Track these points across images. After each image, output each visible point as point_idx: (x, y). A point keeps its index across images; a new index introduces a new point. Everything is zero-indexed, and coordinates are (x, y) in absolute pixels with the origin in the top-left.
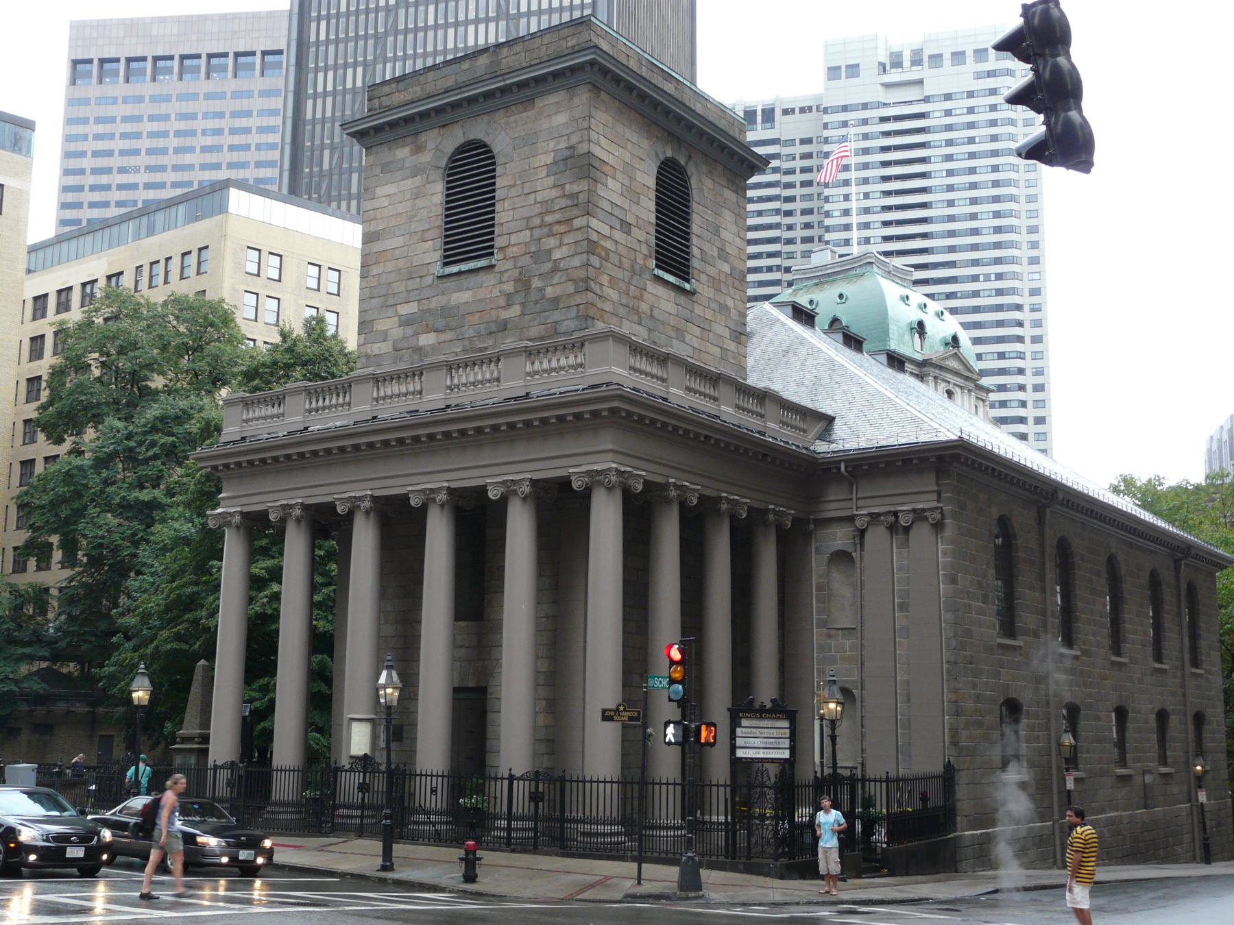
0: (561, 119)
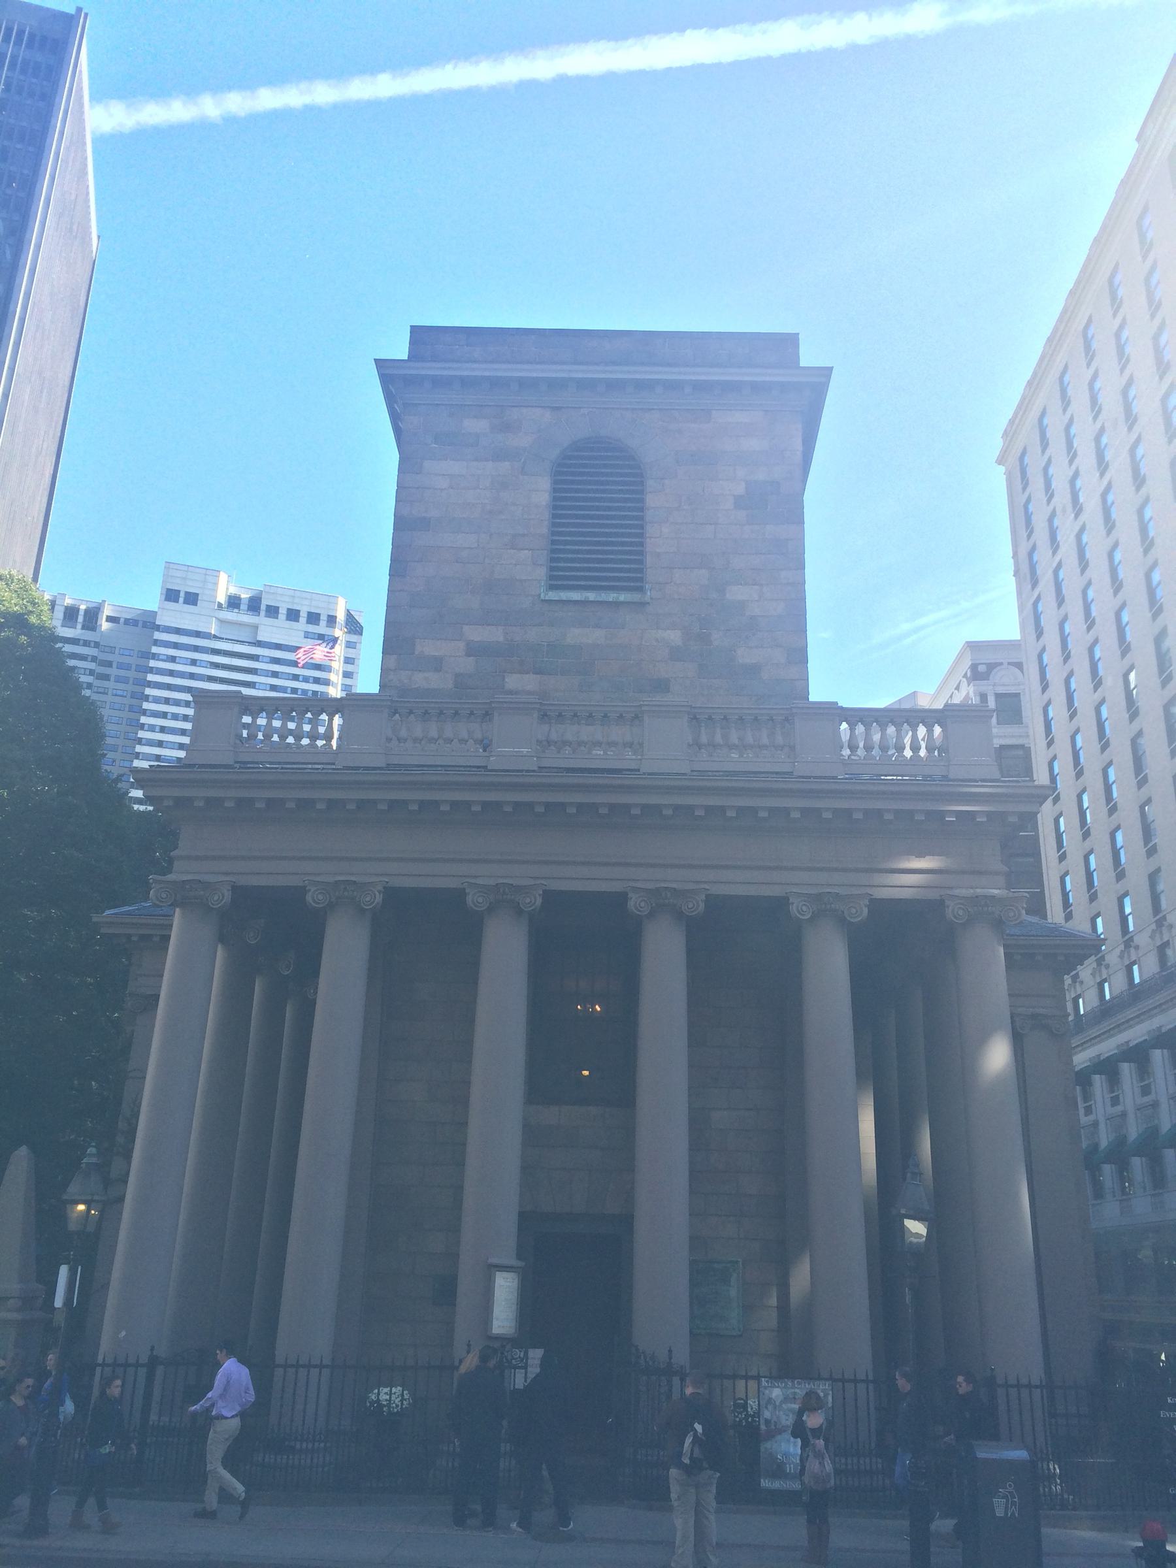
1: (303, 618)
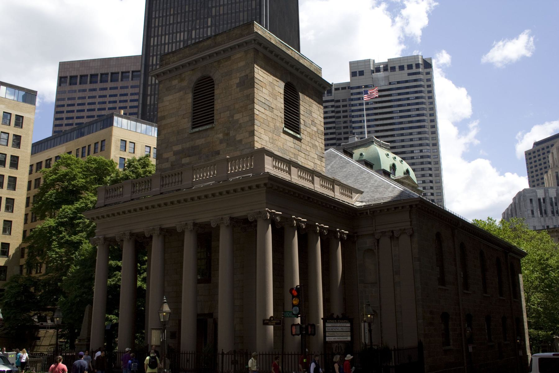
0: (242, 64)
1: (406, 68)
